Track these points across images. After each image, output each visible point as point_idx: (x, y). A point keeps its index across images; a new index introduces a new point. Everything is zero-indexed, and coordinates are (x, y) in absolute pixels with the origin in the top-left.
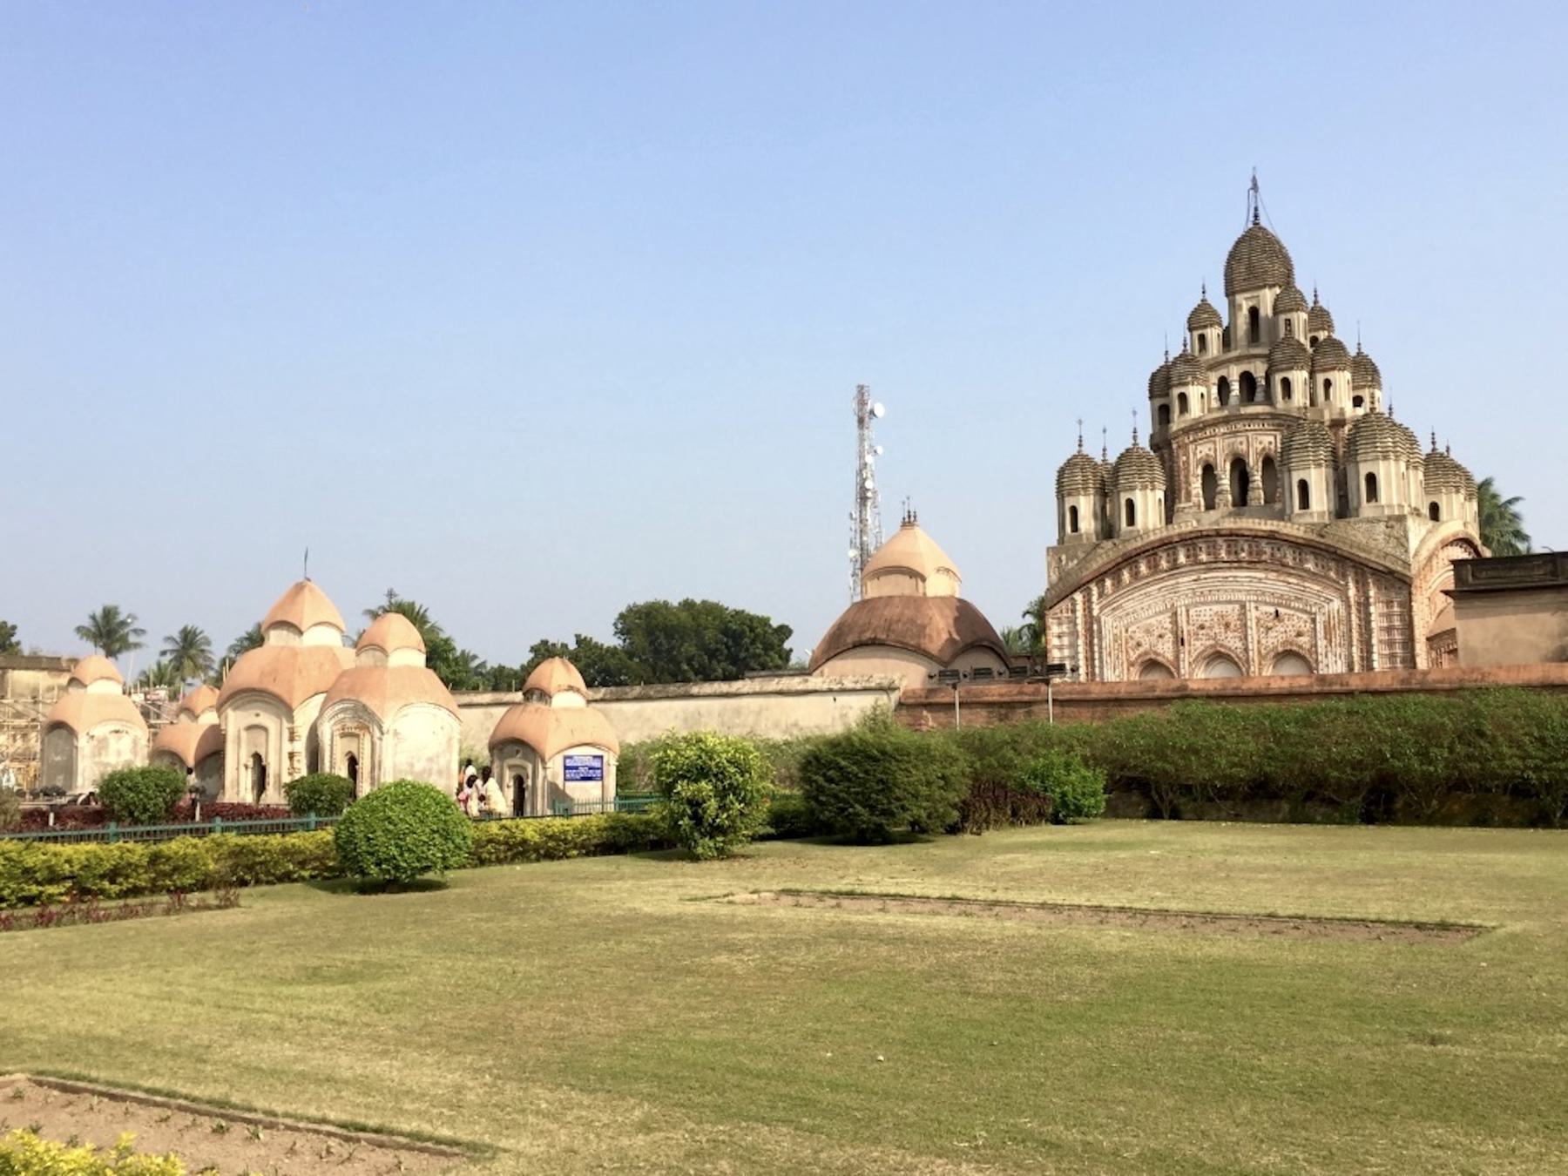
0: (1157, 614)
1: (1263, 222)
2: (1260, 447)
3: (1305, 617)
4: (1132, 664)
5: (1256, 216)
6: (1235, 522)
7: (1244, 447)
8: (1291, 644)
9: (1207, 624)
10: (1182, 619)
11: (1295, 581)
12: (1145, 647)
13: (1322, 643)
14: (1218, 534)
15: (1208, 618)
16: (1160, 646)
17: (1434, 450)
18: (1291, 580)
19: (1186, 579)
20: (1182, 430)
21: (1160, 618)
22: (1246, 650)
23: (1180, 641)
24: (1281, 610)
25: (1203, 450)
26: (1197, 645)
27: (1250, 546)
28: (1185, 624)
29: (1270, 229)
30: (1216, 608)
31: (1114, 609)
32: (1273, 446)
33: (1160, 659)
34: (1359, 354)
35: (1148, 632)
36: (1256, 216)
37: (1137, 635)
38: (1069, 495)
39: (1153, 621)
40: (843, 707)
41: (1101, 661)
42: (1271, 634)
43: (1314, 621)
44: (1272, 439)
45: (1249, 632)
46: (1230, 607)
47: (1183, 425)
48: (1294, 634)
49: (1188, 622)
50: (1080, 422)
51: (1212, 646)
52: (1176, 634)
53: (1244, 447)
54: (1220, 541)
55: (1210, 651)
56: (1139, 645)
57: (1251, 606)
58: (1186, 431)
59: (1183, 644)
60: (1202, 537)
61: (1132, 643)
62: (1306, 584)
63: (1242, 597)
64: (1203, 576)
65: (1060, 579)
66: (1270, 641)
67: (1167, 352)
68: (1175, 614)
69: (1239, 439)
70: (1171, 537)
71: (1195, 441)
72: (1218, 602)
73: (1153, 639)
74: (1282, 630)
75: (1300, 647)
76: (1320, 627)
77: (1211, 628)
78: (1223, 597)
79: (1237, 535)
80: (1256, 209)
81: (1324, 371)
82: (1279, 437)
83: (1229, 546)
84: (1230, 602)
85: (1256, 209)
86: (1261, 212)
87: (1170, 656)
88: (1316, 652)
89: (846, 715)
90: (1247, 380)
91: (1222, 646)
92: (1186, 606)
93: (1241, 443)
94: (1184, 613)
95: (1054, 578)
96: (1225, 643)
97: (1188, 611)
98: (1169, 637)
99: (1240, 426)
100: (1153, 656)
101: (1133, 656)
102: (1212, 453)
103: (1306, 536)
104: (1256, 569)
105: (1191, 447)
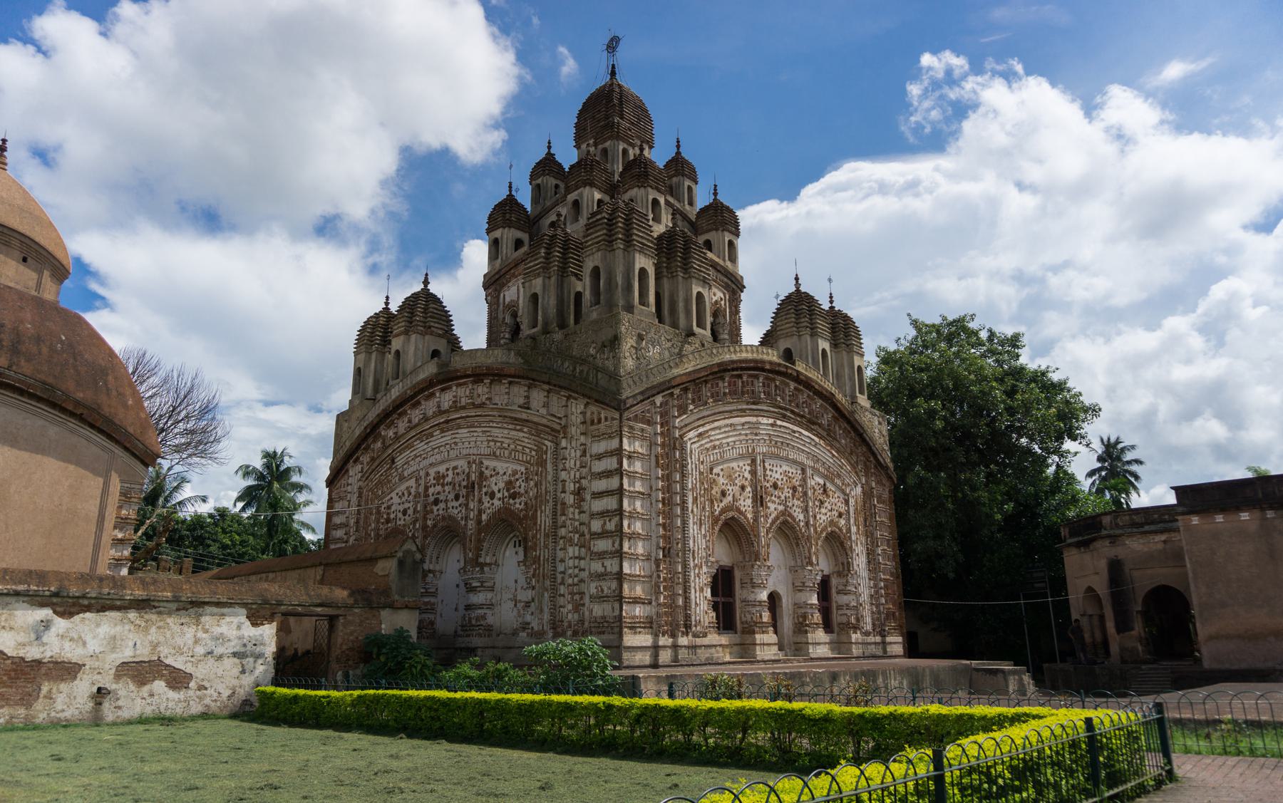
2: (715, 299)
3: (842, 496)
4: (716, 520)
6: (806, 370)
9: (779, 483)
13: (854, 529)
15: (777, 476)
16: (741, 502)
19: (765, 421)
21: (741, 464)
22: (807, 524)
23: (759, 500)
24: (828, 485)
26: (773, 508)
32: (723, 302)
39: (734, 465)
41: (684, 509)
43: (847, 502)
44: (723, 297)
45: (810, 504)
51: (783, 513)
52: (755, 491)
54: (792, 385)
56: (724, 494)
57: (809, 472)
59: (762, 505)
61: (716, 491)
63: (802, 458)
64: (779, 423)
66: (824, 518)
68: (754, 461)
70: (763, 362)
72: (787, 459)
73: (737, 489)
74: (829, 508)
75: (840, 530)
82: (727, 297)
84: (795, 462)
87: (750, 516)
88: (850, 538)
91: (790, 515)
92: (764, 455)
97: (764, 462)
100: (736, 515)
104: (810, 430)
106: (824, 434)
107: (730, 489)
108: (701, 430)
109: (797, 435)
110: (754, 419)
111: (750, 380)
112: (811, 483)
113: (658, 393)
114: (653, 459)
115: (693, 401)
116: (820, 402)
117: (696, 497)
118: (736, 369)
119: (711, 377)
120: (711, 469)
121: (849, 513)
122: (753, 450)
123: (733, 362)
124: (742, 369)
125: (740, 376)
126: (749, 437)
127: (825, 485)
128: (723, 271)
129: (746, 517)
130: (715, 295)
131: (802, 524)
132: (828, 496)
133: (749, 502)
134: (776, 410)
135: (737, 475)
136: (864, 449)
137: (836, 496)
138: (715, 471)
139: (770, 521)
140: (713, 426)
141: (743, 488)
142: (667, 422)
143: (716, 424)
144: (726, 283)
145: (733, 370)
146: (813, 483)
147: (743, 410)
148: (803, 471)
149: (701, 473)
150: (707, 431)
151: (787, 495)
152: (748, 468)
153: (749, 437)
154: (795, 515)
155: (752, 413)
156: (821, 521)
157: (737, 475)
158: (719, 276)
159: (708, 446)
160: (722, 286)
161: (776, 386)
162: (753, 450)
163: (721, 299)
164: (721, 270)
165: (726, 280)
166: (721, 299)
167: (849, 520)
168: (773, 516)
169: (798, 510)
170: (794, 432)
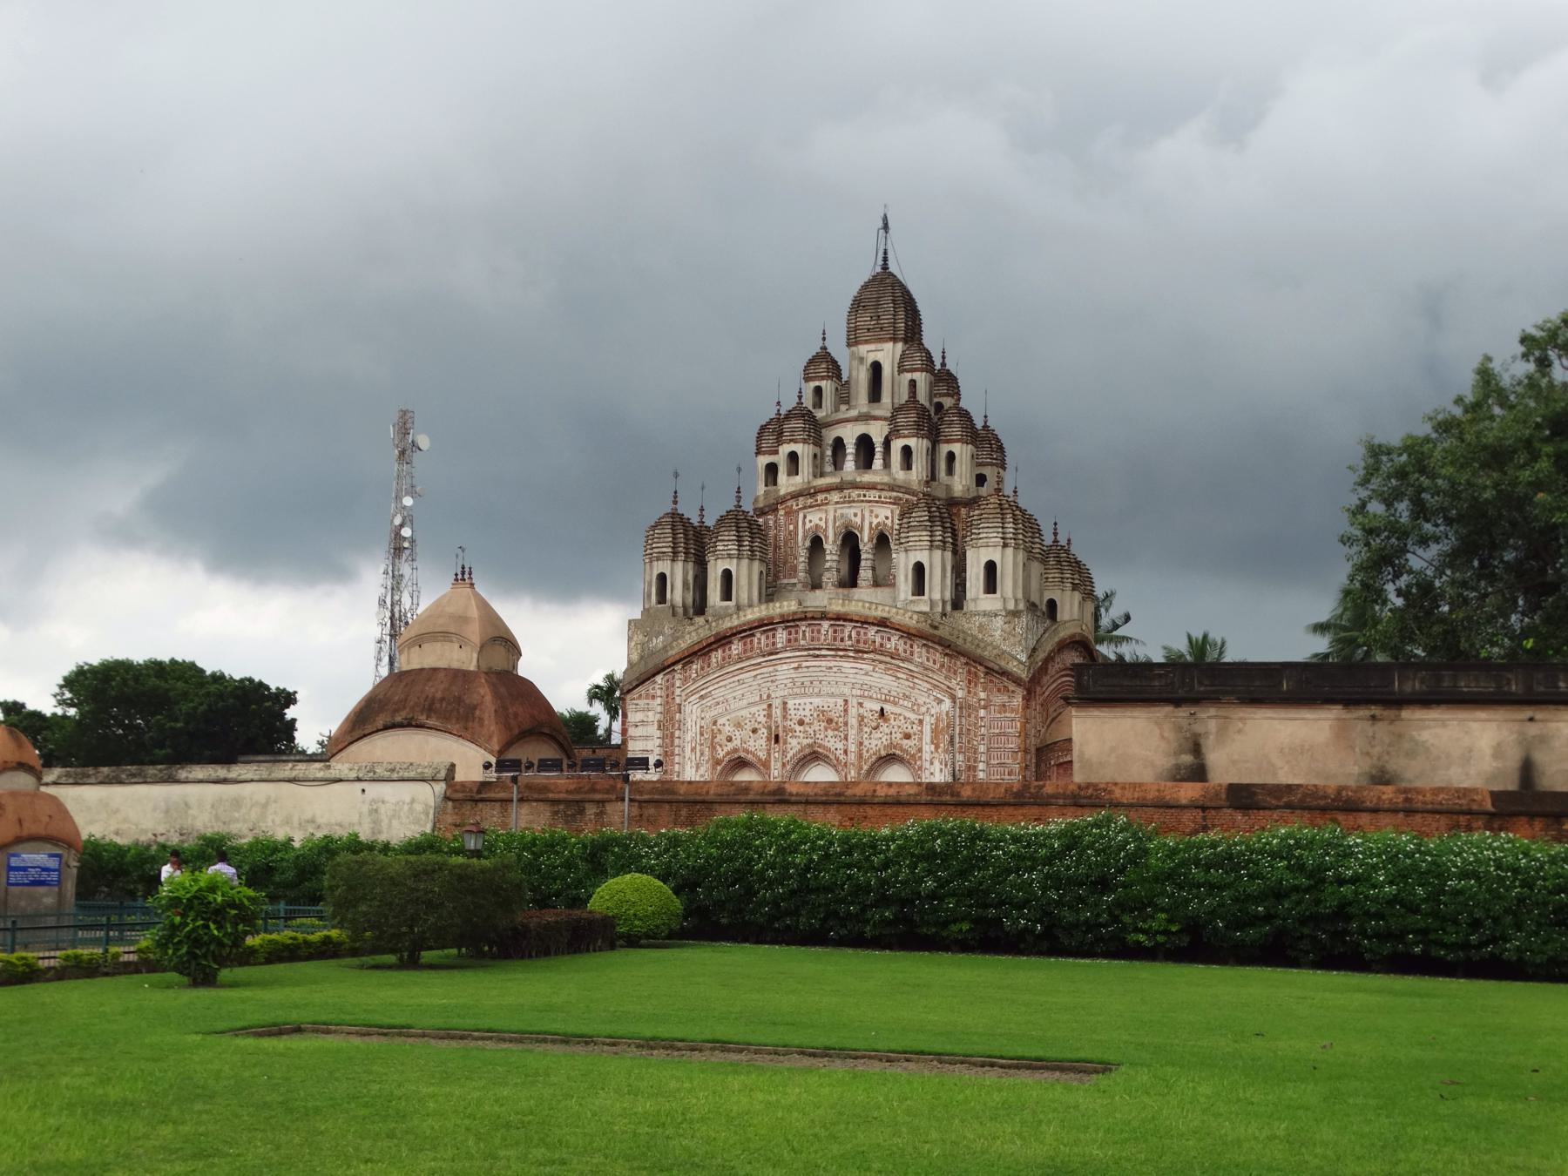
0: (751, 704)
1: (893, 268)
2: (875, 522)
3: (913, 716)
5: (885, 259)
7: (858, 520)
8: (895, 747)
9: (807, 720)
10: (777, 712)
11: (904, 676)
12: (736, 743)
13: (928, 748)
14: (824, 616)
15: (807, 713)
16: (752, 743)
17: (1056, 541)
18: (899, 675)
19: (785, 667)
20: (790, 493)
21: (753, 710)
22: (846, 752)
24: (888, 708)
25: (814, 518)
26: (795, 745)
27: (858, 634)
28: (779, 720)
29: (900, 277)
30: (817, 701)
31: (702, 697)
33: (750, 757)
34: (985, 427)
35: (738, 725)
36: (885, 259)
37: (727, 728)
38: (658, 559)
40: (373, 801)
42: (876, 735)
43: (921, 722)
44: (889, 515)
45: (852, 733)
46: (832, 701)
47: (791, 489)
48: (899, 736)
49: (784, 717)
50: (676, 475)
51: (810, 746)
53: (858, 520)
54: (826, 624)
55: (807, 751)
56: (729, 740)
57: (853, 702)
58: (795, 496)
60: (805, 619)
62: (916, 681)
63: (846, 690)
64: (804, 664)
65: (642, 658)
66: (874, 742)
67: (779, 403)
68: (770, 706)
69: (853, 511)
71: (805, 508)
72: (819, 695)
73: (747, 732)
74: (887, 731)
76: (927, 729)
77: (810, 724)
78: (825, 690)
79: (845, 620)
80: (885, 252)
81: (948, 442)
82: (898, 512)
83: (835, 632)
85: (885, 252)
86: (890, 256)
88: (920, 758)
89: (376, 811)
90: (865, 443)
93: (855, 515)
94: (781, 706)
95: (635, 657)
96: (826, 744)
98: (763, 732)
99: (855, 493)
100: (743, 755)
101: (721, 753)
102: (822, 524)
103: (919, 625)
105: (801, 515)
106: (888, 659)
107: (737, 733)
108: (703, 693)
109: (835, 669)
110: (771, 669)
111: (770, 634)
112: (853, 711)
113: (658, 673)
114: (656, 724)
115: (702, 669)
116: (872, 630)
117: (695, 748)
118: (745, 631)
119: (714, 646)
120: (715, 723)
121: (922, 732)
122: (769, 696)
123: (731, 628)
124: (750, 629)
125: (753, 635)
126: (763, 685)
127: (882, 709)
128: (886, 488)
129: (754, 755)
130: (877, 517)
131: (838, 752)
132: (887, 720)
133: (763, 742)
134: (805, 653)
135: (747, 721)
136: (963, 660)
137: (902, 718)
138: (720, 721)
139: (789, 756)
140: (716, 686)
141: (755, 731)
142: (673, 693)
143: (721, 684)
144: (895, 498)
145: (740, 632)
146: (861, 711)
147: (759, 664)
148: (846, 701)
149: (702, 727)
150: (710, 692)
151: (817, 728)
152: (765, 713)
153: (763, 685)
154: (829, 745)
155: (769, 663)
156: (873, 746)
157: (747, 721)
158: (884, 494)
159: (709, 704)
160: (890, 503)
161: (804, 631)
162: (769, 696)
163: (887, 518)
164: (883, 487)
165: (895, 494)
166: (887, 518)
167: (921, 739)
168: (794, 751)
169: (833, 740)
170: (831, 668)
